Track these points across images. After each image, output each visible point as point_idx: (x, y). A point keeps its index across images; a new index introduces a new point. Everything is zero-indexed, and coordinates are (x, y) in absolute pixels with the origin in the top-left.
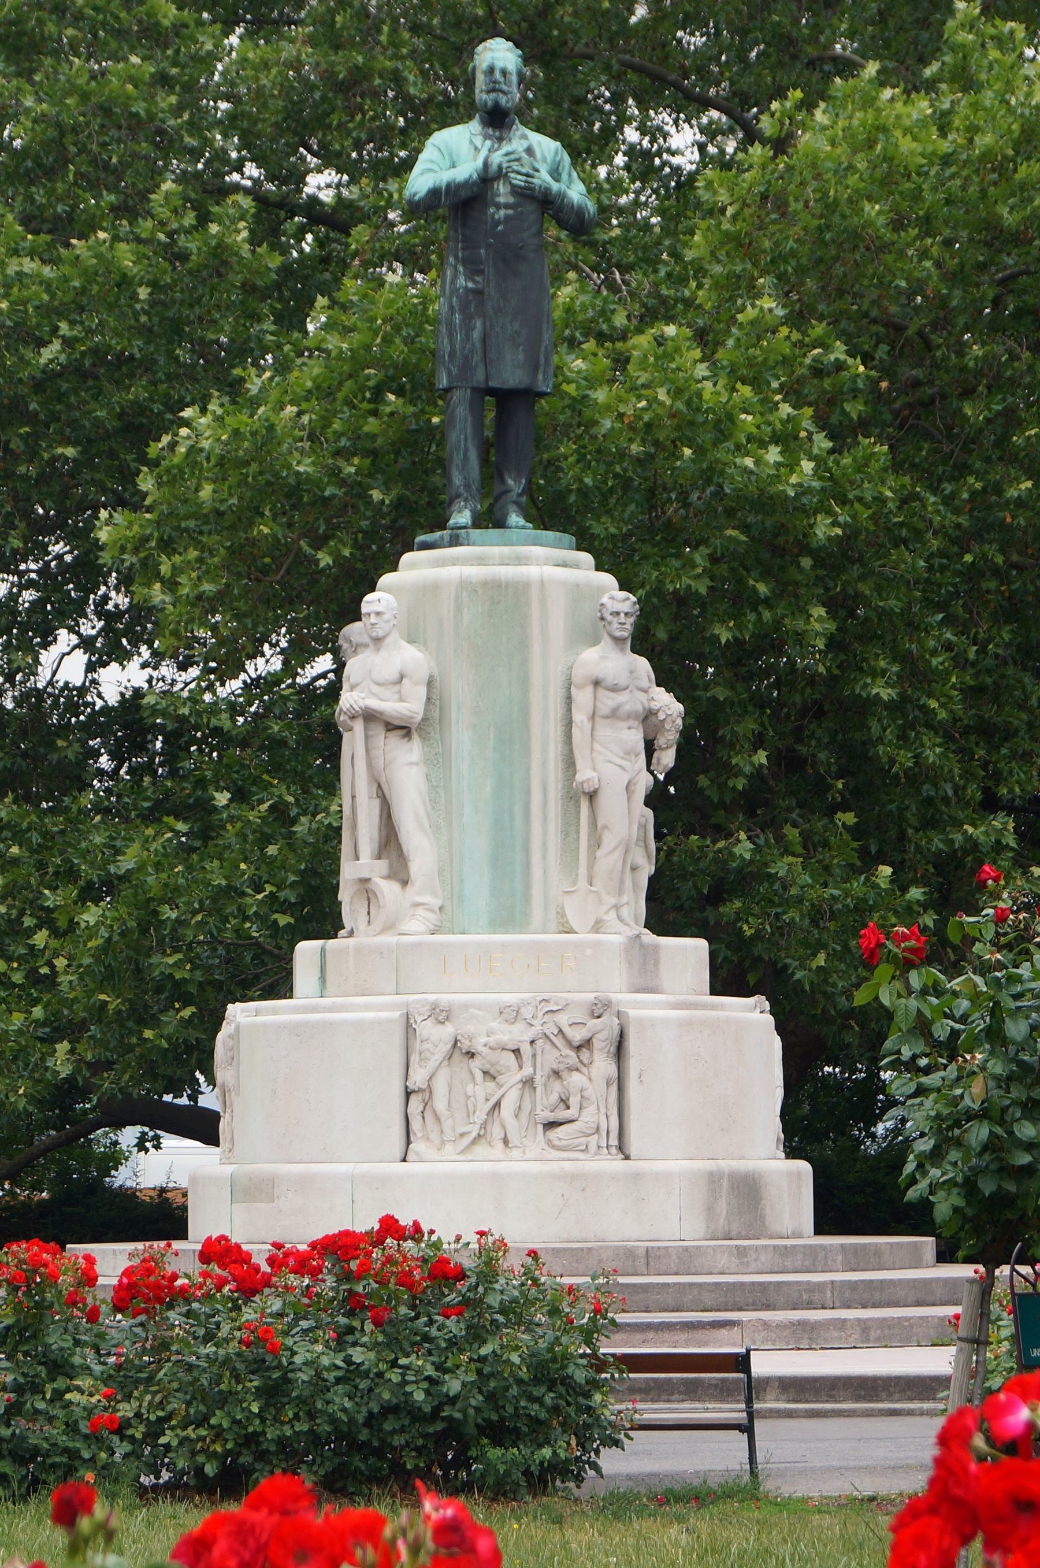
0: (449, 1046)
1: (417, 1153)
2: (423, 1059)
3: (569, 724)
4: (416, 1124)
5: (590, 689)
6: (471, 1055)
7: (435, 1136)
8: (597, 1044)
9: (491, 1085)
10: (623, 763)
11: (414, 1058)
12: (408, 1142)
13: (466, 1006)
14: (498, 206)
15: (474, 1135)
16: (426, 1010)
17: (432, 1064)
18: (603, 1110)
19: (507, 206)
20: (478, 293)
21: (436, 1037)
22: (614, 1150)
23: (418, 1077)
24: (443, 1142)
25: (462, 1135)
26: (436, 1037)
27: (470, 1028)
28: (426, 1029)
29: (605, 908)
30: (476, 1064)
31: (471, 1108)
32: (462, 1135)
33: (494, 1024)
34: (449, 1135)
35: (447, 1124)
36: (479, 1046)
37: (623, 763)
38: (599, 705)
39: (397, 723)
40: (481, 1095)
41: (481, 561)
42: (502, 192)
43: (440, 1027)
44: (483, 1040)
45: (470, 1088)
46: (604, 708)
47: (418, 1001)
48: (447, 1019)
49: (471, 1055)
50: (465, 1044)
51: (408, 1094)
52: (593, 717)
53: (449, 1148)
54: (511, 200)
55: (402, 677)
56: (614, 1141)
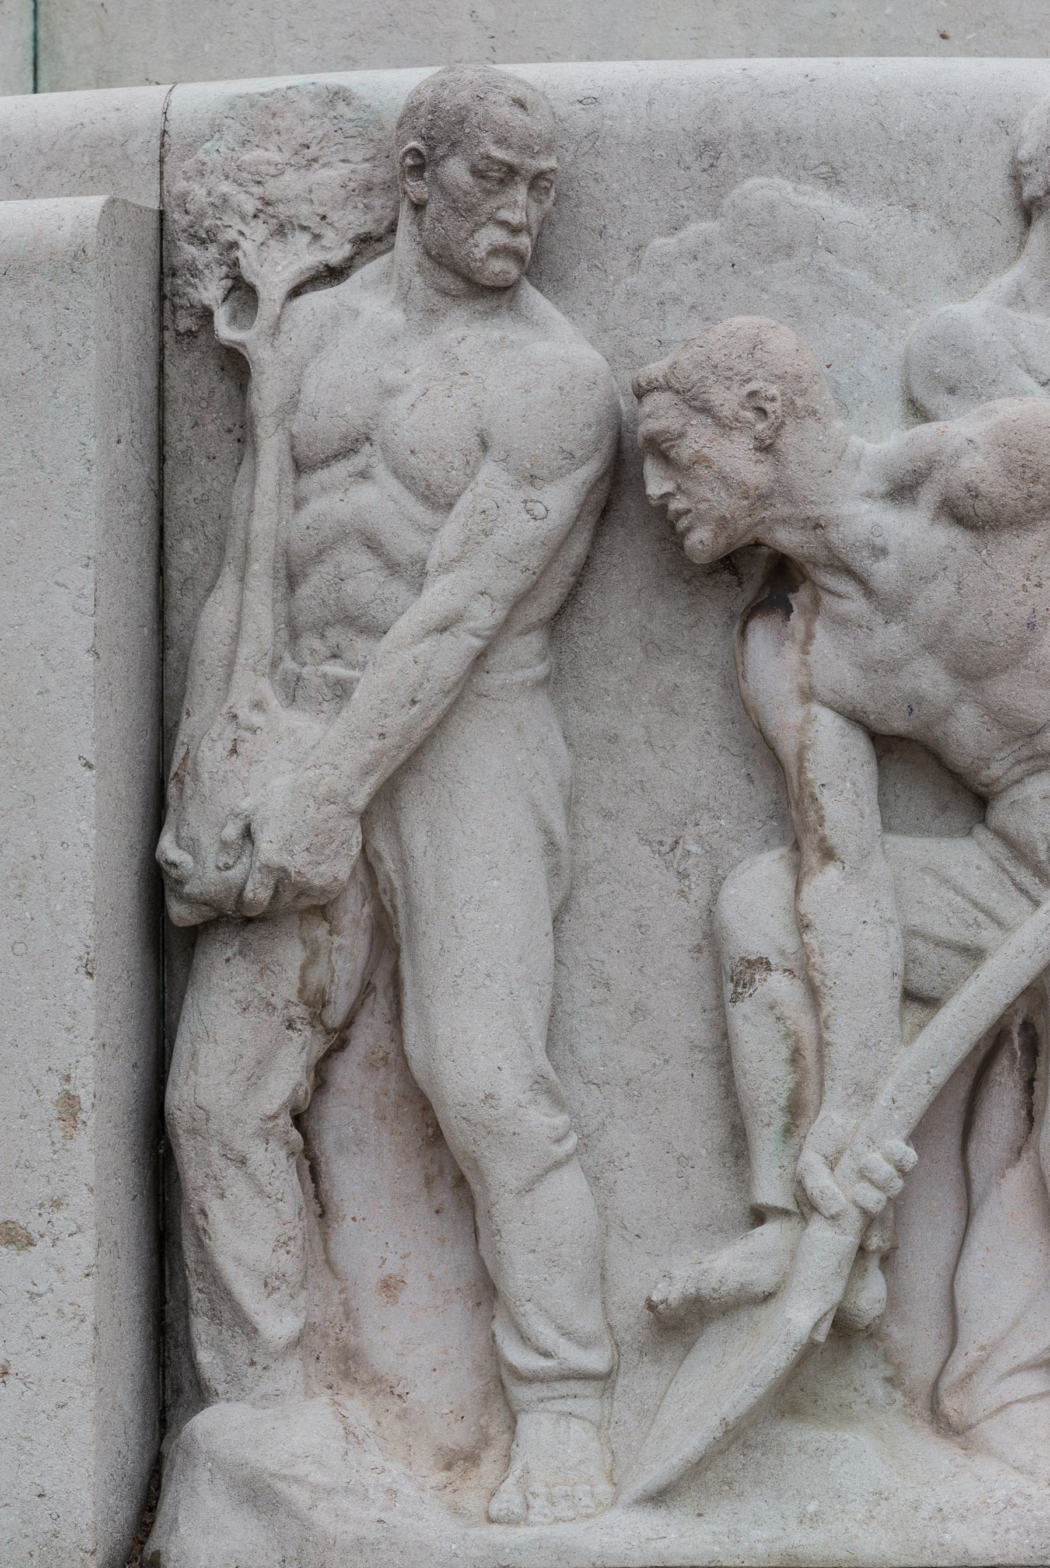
0: (561, 498)
1: (257, 1494)
2: (321, 627)
4: (244, 1227)
6: (764, 578)
7: (419, 1338)
9: (966, 859)
11: (234, 618)
12: (169, 1388)
13: (711, 153)
15: (802, 1315)
16: (329, 187)
17: (402, 664)
21: (435, 414)
23: (274, 783)
24: (501, 1390)
25: (679, 1325)
26: (435, 414)
27: (757, 331)
28: (353, 350)
30: (802, 675)
31: (765, 1075)
32: (679, 1325)
33: (975, 312)
34: (557, 1314)
35: (542, 1223)
36: (847, 480)
40: (862, 961)
43: (468, 333)
44: (885, 441)
45: (756, 895)
47: (261, 119)
48: (538, 265)
49: (764, 578)
50: (718, 481)
51: (172, 938)
53: (554, 1438)
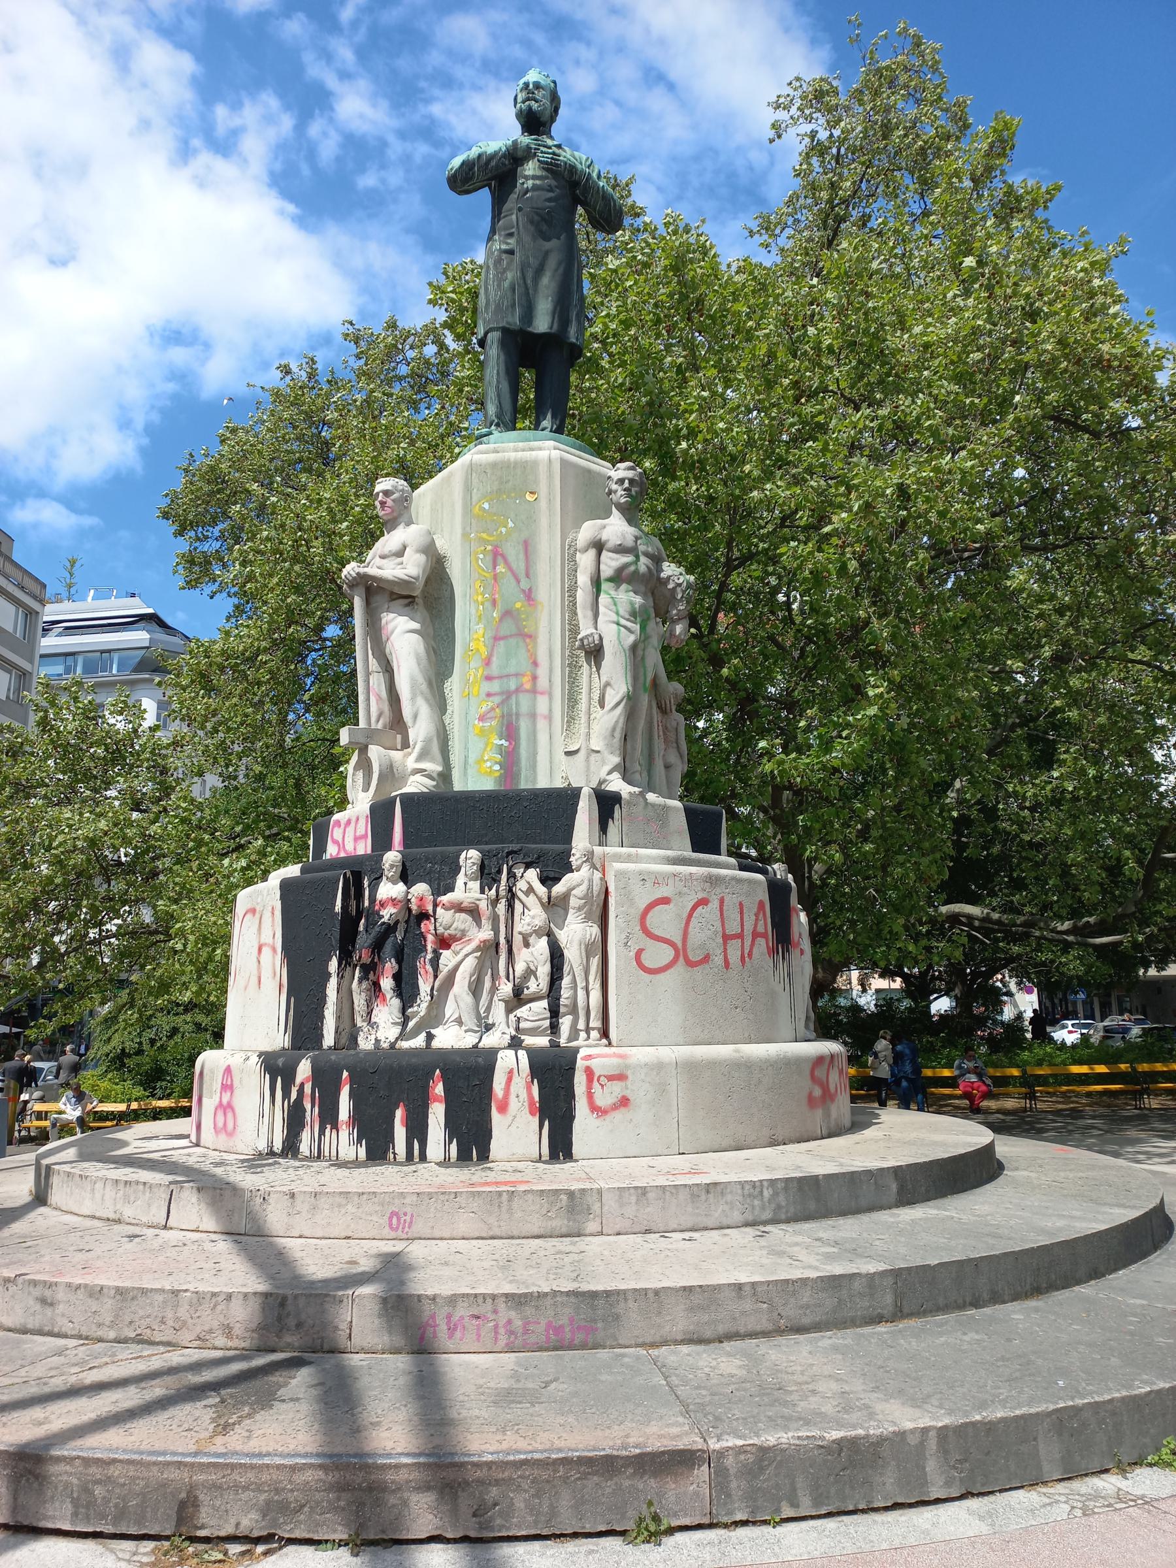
3: (573, 590)
5: (592, 553)
8: (574, 902)
10: (629, 624)
14: (527, 178)
18: (581, 984)
19: (534, 177)
20: (511, 252)
22: (595, 1034)
29: (607, 768)
37: (629, 624)
38: (602, 567)
39: (396, 590)
41: (496, 451)
42: (531, 168)
46: (607, 570)
52: (597, 582)
54: (539, 173)
55: (405, 547)
56: (595, 1023)
